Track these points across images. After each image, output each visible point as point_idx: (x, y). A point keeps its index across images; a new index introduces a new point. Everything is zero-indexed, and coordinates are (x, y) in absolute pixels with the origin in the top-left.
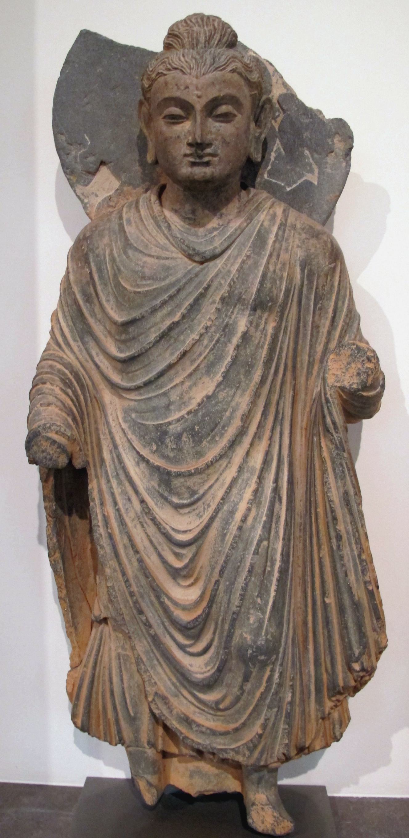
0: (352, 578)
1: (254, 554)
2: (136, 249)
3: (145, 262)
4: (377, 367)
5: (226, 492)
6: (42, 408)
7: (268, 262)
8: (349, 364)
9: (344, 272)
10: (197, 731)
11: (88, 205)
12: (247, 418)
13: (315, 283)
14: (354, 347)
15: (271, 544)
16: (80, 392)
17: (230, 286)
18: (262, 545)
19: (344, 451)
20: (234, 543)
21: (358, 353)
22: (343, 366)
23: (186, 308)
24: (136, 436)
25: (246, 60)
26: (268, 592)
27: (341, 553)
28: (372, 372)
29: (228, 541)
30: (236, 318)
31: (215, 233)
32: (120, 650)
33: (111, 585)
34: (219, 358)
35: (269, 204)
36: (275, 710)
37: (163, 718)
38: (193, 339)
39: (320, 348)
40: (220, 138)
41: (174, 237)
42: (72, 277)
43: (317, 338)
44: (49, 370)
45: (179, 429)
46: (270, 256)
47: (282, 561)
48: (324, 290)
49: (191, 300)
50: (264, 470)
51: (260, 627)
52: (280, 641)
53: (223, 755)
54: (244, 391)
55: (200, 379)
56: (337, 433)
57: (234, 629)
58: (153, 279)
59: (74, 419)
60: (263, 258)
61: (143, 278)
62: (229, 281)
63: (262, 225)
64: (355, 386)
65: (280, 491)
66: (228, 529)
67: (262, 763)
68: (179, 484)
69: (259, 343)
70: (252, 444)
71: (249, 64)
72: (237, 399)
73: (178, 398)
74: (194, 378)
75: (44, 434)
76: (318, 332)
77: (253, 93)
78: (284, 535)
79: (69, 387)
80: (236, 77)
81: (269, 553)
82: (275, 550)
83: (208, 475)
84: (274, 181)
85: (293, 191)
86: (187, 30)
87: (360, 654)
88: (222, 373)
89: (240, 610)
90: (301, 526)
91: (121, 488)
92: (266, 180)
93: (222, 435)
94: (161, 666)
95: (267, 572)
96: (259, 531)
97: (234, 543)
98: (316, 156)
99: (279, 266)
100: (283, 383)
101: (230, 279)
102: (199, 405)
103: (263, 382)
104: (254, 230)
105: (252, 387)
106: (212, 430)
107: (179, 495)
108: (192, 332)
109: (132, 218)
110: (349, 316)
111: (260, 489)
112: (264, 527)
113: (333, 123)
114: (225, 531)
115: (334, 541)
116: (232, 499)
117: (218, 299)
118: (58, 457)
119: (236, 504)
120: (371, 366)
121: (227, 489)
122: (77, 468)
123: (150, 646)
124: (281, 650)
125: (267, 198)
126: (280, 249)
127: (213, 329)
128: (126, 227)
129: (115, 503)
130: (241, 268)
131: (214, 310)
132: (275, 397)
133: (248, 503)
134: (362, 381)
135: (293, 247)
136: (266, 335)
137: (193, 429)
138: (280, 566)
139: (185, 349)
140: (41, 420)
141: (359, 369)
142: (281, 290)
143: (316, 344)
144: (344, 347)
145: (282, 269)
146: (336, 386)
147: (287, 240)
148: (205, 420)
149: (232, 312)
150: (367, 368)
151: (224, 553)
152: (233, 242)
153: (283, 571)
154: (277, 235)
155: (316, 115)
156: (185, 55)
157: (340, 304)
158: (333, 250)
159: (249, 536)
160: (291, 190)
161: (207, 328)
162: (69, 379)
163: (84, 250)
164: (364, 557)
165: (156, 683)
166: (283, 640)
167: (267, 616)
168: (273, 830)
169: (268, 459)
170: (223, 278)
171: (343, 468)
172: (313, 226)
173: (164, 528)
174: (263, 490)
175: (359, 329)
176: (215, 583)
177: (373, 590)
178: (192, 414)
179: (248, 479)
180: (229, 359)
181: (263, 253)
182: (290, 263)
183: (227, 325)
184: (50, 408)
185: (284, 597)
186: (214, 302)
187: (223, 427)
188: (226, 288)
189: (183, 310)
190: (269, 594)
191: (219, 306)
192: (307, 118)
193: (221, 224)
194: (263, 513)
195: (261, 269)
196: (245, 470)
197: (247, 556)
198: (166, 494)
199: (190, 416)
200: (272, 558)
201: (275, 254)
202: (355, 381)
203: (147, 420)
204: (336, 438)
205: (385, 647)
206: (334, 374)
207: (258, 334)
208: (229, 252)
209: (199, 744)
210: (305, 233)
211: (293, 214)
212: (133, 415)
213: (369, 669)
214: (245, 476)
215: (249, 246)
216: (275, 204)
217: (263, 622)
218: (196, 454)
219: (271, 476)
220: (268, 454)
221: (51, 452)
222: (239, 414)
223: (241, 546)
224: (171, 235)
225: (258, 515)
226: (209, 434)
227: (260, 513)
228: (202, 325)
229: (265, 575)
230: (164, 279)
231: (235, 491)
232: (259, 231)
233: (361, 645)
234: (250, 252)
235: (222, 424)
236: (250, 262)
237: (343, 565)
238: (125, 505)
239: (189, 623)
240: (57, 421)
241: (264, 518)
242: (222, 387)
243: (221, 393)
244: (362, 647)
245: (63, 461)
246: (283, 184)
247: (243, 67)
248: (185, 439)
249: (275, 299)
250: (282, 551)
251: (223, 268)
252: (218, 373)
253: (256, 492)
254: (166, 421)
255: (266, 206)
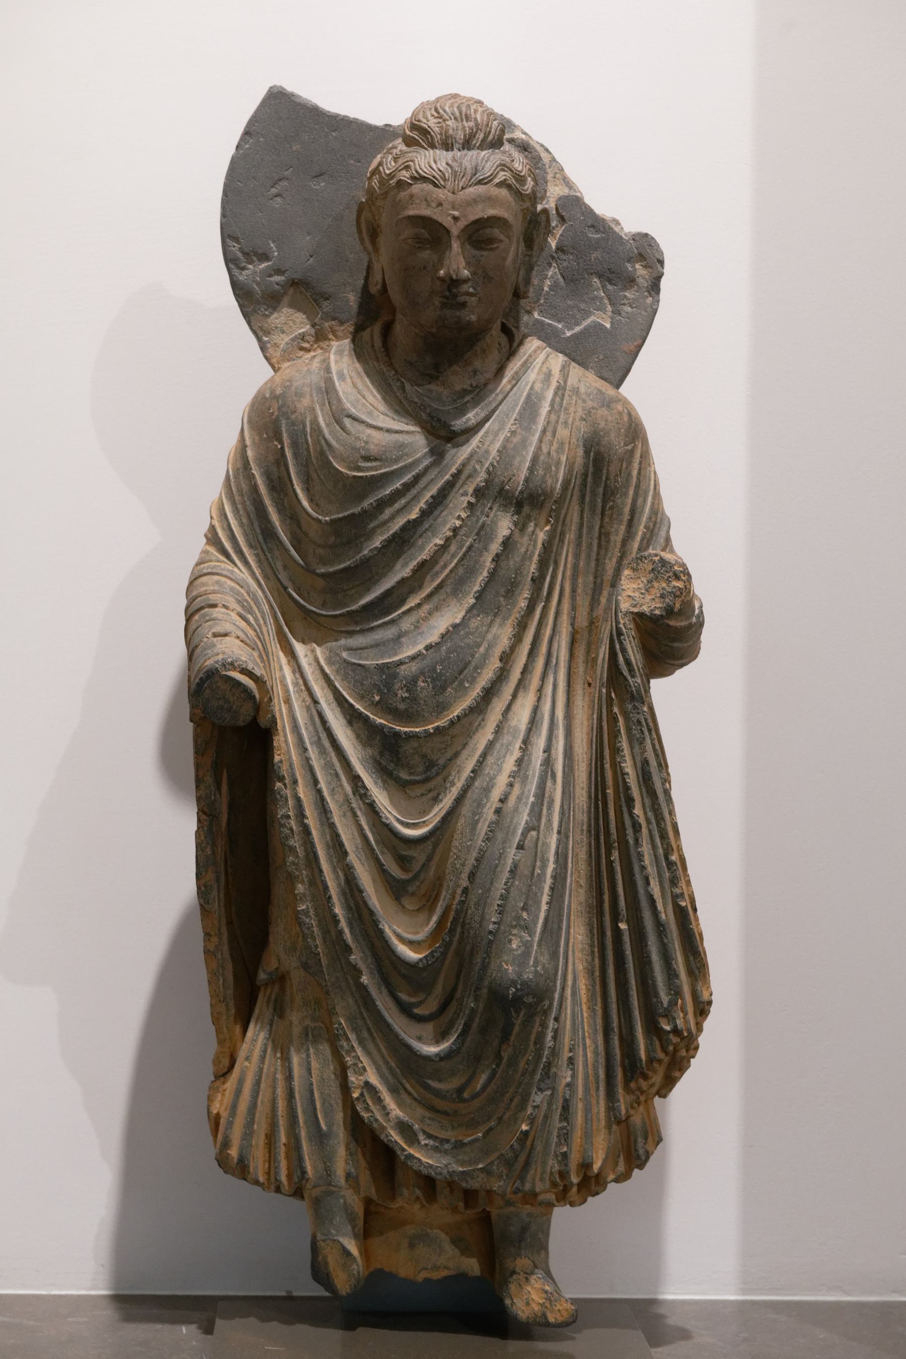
0: (655, 888)
1: (517, 848)
2: (355, 419)
3: (369, 436)
4: (688, 587)
5: (478, 761)
6: (215, 639)
7: (540, 441)
8: (650, 582)
9: (646, 455)
10: (426, 1145)
11: (269, 345)
12: (506, 658)
13: (605, 471)
14: (656, 559)
15: (541, 836)
16: (262, 622)
17: (488, 472)
18: (529, 836)
19: (643, 703)
20: (490, 831)
21: (662, 566)
22: (641, 586)
23: (427, 501)
24: (349, 683)
25: (516, 165)
26: (538, 903)
27: (640, 849)
28: (682, 593)
29: (481, 829)
30: (495, 516)
31: (467, 398)
32: (308, 1022)
33: (304, 907)
34: (472, 572)
35: (542, 357)
36: (549, 1092)
37: (375, 1125)
38: (436, 545)
39: (610, 566)
40: (480, 272)
41: (411, 402)
42: (250, 453)
43: (607, 549)
44: (216, 588)
45: (414, 669)
46: (544, 432)
47: (556, 861)
48: (617, 481)
49: (434, 490)
50: (532, 732)
51: (527, 954)
52: (555, 982)
53: (467, 1182)
54: (505, 619)
55: (444, 600)
56: (633, 676)
57: (490, 958)
58: (381, 460)
59: (260, 656)
60: (533, 435)
61: (367, 459)
62: (487, 465)
63: (532, 388)
64: (657, 612)
65: (553, 765)
66: (481, 812)
67: (528, 1186)
68: (411, 751)
69: (526, 552)
70: (514, 696)
71: (521, 172)
72: (494, 630)
73: (412, 627)
74: (435, 599)
75: (224, 673)
76: (608, 542)
77: (525, 206)
78: (560, 826)
79: (250, 613)
80: (504, 192)
81: (539, 848)
82: (546, 845)
83: (454, 737)
84: (547, 321)
85: (575, 337)
86: (439, 123)
87: (670, 1002)
88: (475, 593)
89: (499, 928)
90: (582, 826)
91: (325, 759)
92: (537, 320)
93: (473, 681)
94: (373, 1039)
95: (536, 874)
96: (524, 817)
97: (490, 831)
98: (609, 287)
99: (555, 445)
100: (557, 614)
101: (488, 463)
102: (443, 636)
103: (531, 609)
104: (521, 396)
105: (516, 615)
106: (461, 672)
107: (410, 769)
108: (434, 535)
109: (345, 371)
110: (653, 519)
111: (526, 758)
112: (532, 810)
113: (634, 240)
114: (477, 818)
115: (630, 831)
116: (487, 772)
117: (471, 490)
118: (241, 707)
119: (492, 779)
120: (679, 584)
121: (481, 756)
122: (263, 727)
123: (358, 1006)
124: (557, 996)
125: (538, 348)
126: (557, 422)
127: (462, 532)
128: (337, 384)
129: (316, 782)
130: (504, 447)
131: (465, 504)
132: (548, 632)
133: (510, 776)
134: (669, 606)
135: (574, 419)
136: (535, 542)
137: (434, 669)
138: (555, 869)
139: (424, 558)
140: (218, 654)
141: (663, 589)
142: (557, 481)
143: (605, 559)
144: (643, 559)
145: (560, 450)
146: (632, 613)
147: (566, 409)
148: (449, 658)
149: (491, 508)
150: (675, 587)
151: (475, 847)
152: (494, 411)
153: (559, 878)
154: (552, 405)
155: (610, 228)
156: (437, 159)
157: (640, 501)
158: (630, 425)
159: (511, 822)
160: (571, 335)
161: (455, 530)
162: (247, 601)
163: (273, 414)
164: (674, 858)
165: (364, 1069)
166: (559, 982)
167: (537, 939)
168: (544, 1315)
169: (537, 718)
170: (479, 462)
171: (642, 726)
172: (604, 390)
173: (387, 818)
174: (530, 760)
175: (668, 540)
176: (463, 892)
177: (686, 906)
178: (433, 650)
179: (510, 744)
180: (485, 574)
181: (534, 427)
182: (570, 443)
183: (483, 526)
184: (227, 638)
185: (560, 916)
186: (465, 494)
187: (476, 668)
188: (483, 476)
189: (422, 504)
190: (539, 908)
191: (473, 500)
192: (598, 231)
193: (474, 385)
194: (529, 791)
195: (532, 449)
196: (505, 731)
197: (508, 850)
198: (391, 766)
199: (430, 651)
200: (543, 857)
201: (550, 429)
202: (658, 605)
203: (367, 659)
204: (632, 684)
205: (710, 1003)
206: (630, 596)
207: (526, 539)
208: (487, 425)
209: (431, 1166)
210: (592, 400)
211: (575, 371)
212: (345, 655)
213: (686, 1034)
214: (505, 739)
215: (513, 418)
216: (550, 357)
217: (532, 946)
218: (437, 707)
219: (540, 742)
220: (536, 710)
221: (231, 699)
222: (498, 651)
223: (500, 836)
224: (406, 398)
225: (523, 793)
226: (456, 678)
227: (526, 792)
228: (448, 526)
229: (535, 880)
230: (396, 461)
231: (490, 760)
232: (529, 396)
233: (671, 990)
234: (515, 427)
235: (473, 664)
236: (515, 440)
237: (643, 868)
238: (330, 783)
239: (421, 960)
240: (241, 655)
241: (532, 799)
242: (475, 612)
243: (473, 620)
244: (672, 992)
245: (245, 715)
246: (560, 326)
247: (513, 177)
248: (423, 684)
249: (549, 492)
250: (558, 848)
251: (478, 447)
252: (470, 593)
253: (519, 762)
254: (396, 658)
255: (537, 360)
